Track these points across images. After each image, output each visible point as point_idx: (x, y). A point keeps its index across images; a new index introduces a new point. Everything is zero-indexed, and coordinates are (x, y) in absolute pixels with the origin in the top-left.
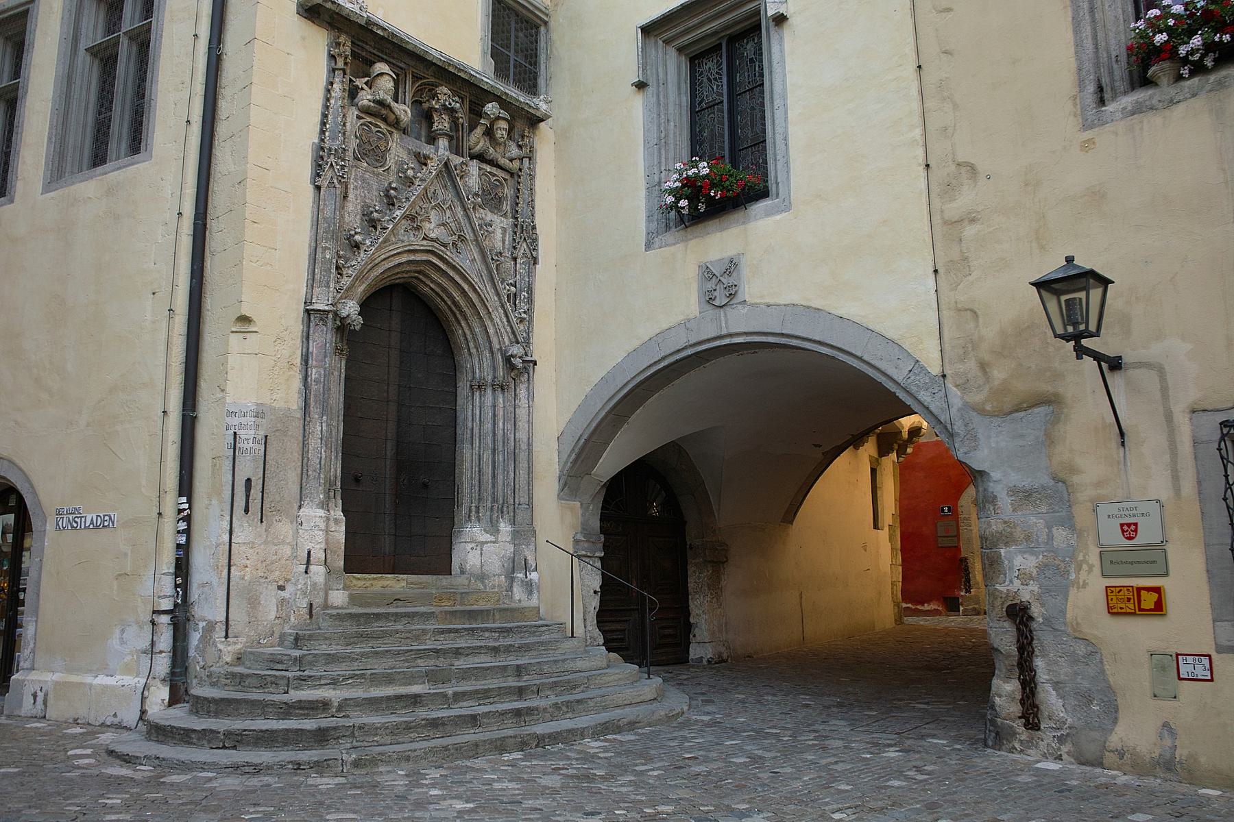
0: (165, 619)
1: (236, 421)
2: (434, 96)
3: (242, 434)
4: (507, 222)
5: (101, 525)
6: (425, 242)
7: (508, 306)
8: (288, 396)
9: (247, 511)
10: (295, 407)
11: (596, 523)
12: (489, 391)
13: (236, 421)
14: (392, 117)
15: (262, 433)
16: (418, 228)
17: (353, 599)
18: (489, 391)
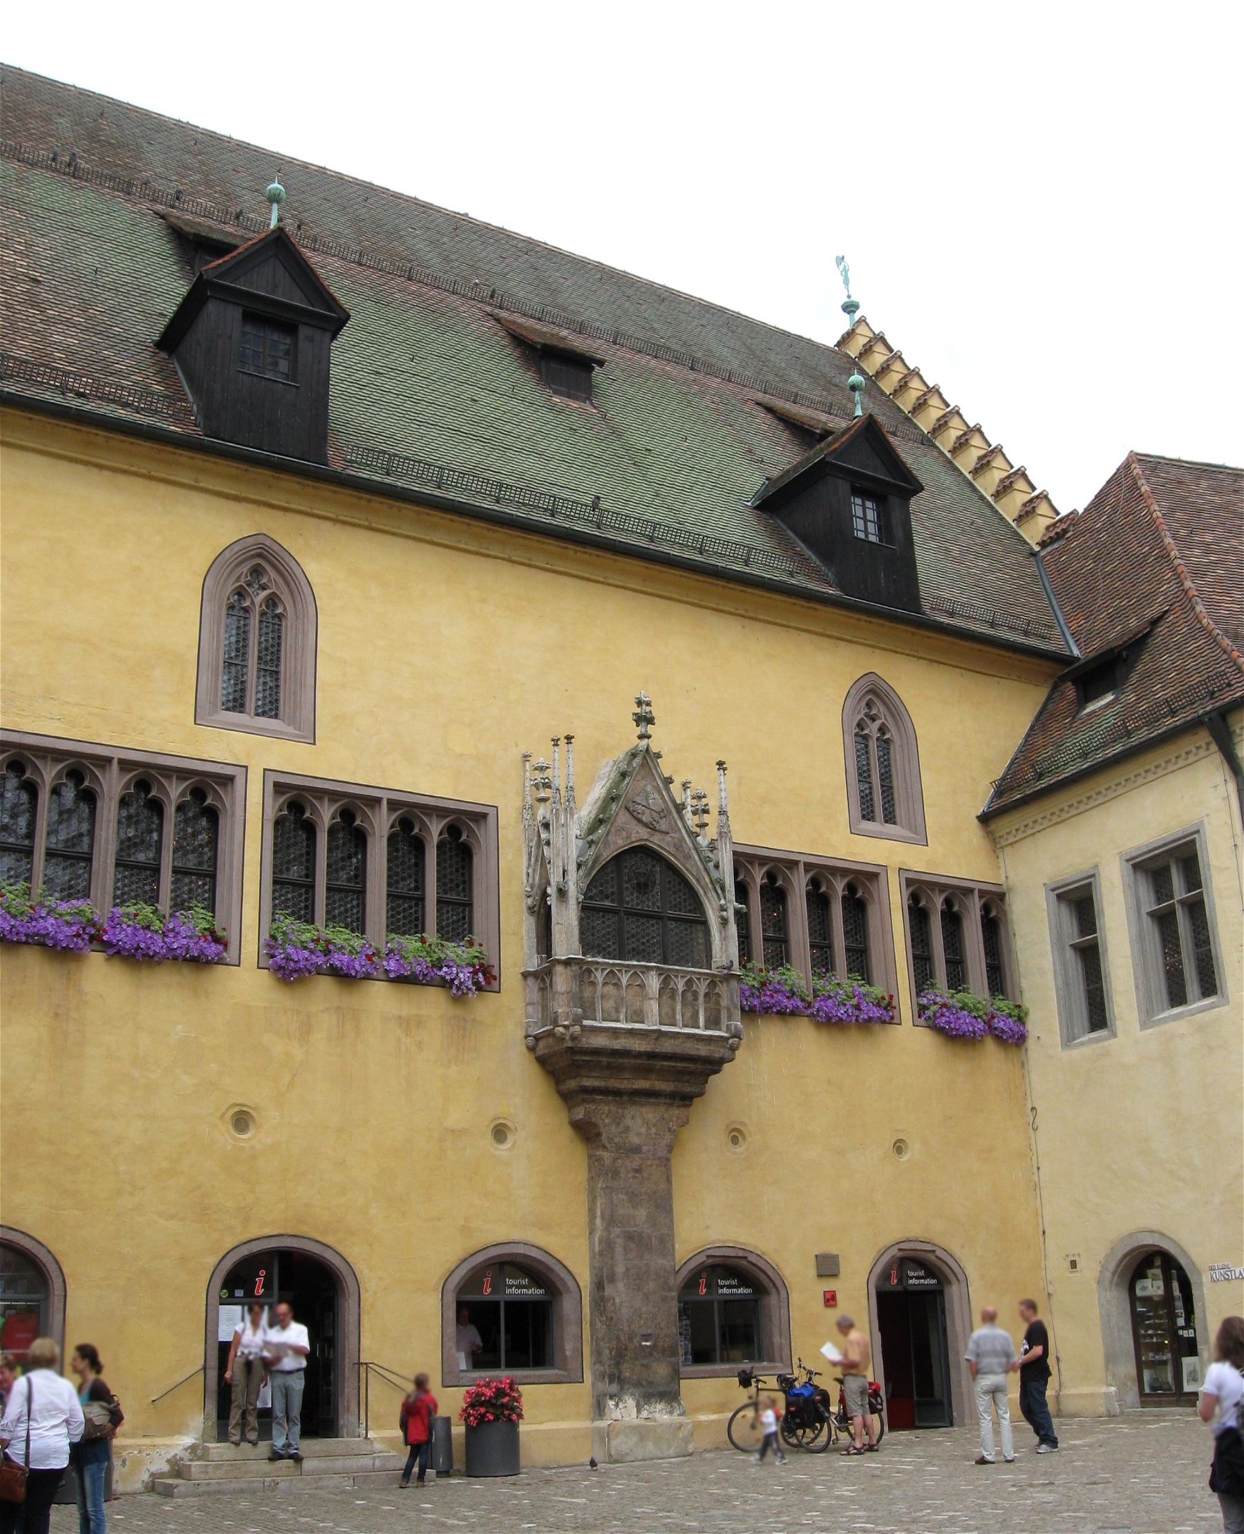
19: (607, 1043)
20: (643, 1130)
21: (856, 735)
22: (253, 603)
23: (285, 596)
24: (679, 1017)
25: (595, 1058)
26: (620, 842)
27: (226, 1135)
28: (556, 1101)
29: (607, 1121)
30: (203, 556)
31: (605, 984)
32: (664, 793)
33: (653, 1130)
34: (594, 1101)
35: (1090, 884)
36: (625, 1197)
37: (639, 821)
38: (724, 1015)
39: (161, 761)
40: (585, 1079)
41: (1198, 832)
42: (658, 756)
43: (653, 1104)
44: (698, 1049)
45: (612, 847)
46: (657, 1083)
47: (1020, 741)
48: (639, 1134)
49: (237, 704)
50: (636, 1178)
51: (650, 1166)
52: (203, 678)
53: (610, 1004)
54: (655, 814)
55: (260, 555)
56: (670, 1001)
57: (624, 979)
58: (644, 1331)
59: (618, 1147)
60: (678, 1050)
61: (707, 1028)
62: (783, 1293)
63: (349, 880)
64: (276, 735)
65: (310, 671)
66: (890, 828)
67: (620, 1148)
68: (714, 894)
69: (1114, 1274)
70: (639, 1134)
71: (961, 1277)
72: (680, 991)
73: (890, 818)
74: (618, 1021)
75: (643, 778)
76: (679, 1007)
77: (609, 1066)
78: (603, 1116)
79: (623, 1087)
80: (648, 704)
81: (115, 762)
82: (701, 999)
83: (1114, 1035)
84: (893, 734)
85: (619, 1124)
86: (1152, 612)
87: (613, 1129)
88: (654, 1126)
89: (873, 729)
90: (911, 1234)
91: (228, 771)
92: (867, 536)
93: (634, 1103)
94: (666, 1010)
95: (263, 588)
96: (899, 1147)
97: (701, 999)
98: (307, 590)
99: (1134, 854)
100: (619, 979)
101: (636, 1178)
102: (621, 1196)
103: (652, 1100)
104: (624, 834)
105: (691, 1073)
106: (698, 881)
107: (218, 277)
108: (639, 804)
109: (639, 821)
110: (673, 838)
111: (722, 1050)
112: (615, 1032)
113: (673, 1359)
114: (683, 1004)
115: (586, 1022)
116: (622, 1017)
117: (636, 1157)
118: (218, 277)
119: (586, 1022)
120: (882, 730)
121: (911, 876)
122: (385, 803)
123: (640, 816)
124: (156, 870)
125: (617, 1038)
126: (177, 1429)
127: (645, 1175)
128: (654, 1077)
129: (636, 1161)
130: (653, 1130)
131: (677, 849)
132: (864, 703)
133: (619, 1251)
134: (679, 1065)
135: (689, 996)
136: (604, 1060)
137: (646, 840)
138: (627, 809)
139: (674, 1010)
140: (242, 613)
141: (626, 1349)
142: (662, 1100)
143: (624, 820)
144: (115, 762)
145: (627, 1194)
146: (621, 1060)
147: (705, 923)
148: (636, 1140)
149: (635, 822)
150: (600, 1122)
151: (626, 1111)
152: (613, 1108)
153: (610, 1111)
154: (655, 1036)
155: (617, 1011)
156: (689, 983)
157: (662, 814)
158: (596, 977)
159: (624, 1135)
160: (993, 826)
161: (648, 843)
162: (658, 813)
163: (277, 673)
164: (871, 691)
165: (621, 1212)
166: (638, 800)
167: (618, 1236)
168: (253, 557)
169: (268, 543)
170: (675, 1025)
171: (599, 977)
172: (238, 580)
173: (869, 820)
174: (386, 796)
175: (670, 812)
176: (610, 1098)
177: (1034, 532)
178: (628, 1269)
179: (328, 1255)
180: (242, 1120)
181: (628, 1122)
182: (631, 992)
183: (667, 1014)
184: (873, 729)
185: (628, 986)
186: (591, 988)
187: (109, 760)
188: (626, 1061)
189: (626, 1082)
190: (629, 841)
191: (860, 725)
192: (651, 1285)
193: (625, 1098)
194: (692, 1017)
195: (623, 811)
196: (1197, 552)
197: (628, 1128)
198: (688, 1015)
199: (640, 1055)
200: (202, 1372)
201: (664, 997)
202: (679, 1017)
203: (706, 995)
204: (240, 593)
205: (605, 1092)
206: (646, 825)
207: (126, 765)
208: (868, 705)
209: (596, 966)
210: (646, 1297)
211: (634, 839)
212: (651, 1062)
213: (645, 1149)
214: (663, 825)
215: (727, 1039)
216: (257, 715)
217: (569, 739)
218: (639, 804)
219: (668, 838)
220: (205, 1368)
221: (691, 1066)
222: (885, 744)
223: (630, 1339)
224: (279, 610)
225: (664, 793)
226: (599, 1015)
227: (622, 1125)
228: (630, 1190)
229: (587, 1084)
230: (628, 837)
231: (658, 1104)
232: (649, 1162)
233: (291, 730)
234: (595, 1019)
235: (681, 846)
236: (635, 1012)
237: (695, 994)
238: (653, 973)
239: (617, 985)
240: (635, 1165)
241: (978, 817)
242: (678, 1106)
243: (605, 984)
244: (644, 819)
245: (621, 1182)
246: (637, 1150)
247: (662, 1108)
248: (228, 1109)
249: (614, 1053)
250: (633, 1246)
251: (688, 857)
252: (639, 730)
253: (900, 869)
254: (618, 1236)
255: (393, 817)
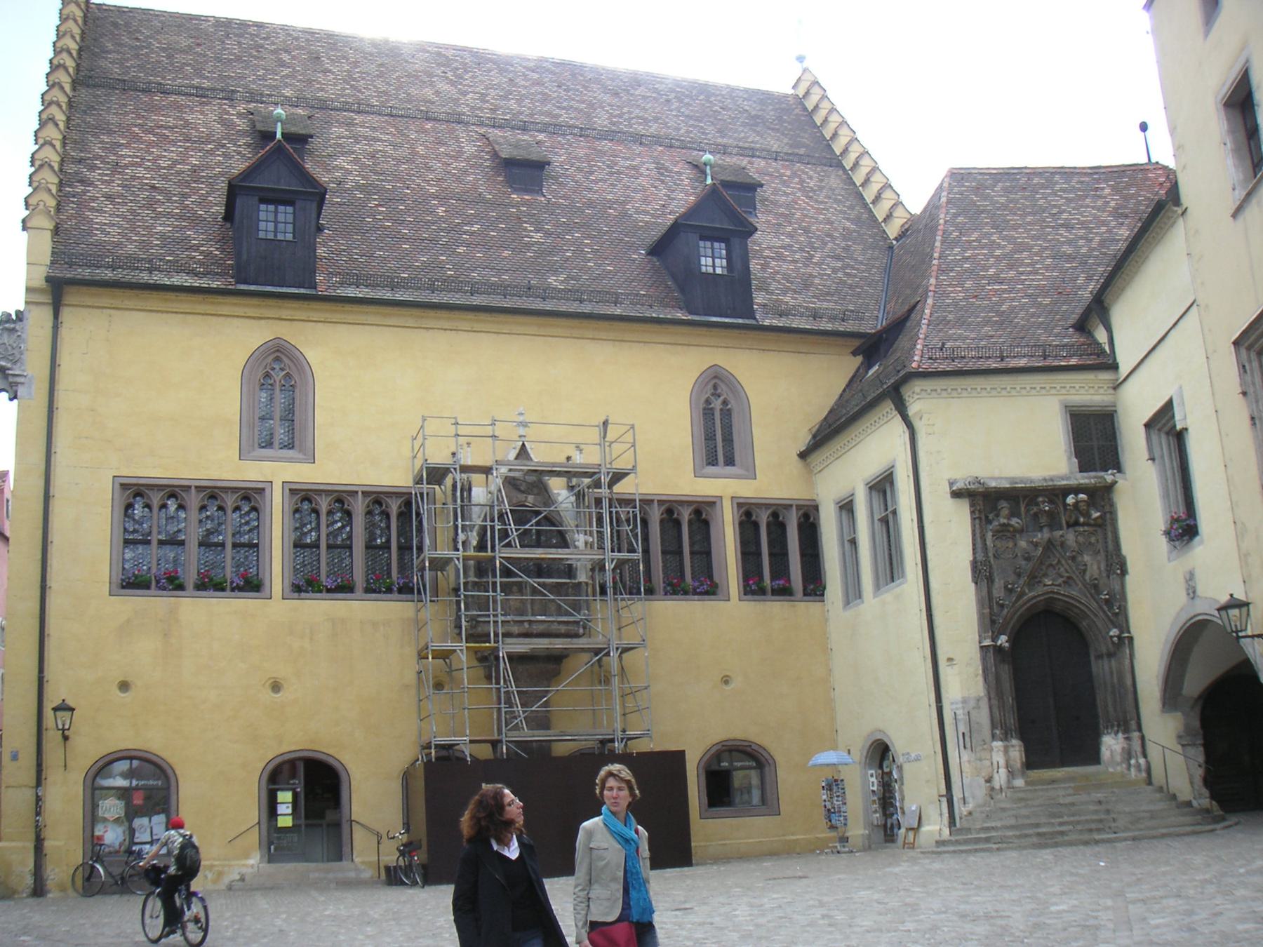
0: (944, 800)
1: (954, 706)
2: (1037, 504)
3: (958, 712)
4: (1101, 557)
5: (917, 759)
6: (1046, 588)
7: (1105, 608)
8: (977, 687)
9: (965, 747)
10: (982, 694)
11: (1196, 723)
12: (1105, 658)
13: (954, 706)
14: (1011, 529)
15: (966, 711)
16: (1040, 582)
17: (1027, 783)
18: (1105, 658)
21: (704, 409)
22: (275, 381)
23: (296, 376)
27: (268, 696)
30: (241, 358)
35: (852, 501)
39: (219, 484)
41: (893, 466)
47: (837, 397)
49: (269, 445)
52: (244, 430)
55: (278, 351)
63: (343, 540)
64: (290, 460)
65: (311, 419)
66: (729, 469)
69: (866, 758)
71: (771, 761)
73: (730, 461)
81: (193, 488)
83: (863, 602)
84: (733, 404)
86: (913, 302)
89: (717, 404)
90: (731, 736)
91: (260, 485)
92: (714, 270)
95: (282, 369)
96: (726, 681)
98: (307, 368)
99: (870, 480)
107: (242, 181)
118: (242, 181)
120: (725, 403)
121: (741, 501)
122: (360, 493)
124: (223, 545)
126: (247, 857)
132: (710, 386)
140: (269, 387)
144: (193, 488)
160: (809, 460)
163: (293, 421)
164: (715, 377)
168: (278, 351)
169: (283, 342)
172: (265, 368)
173: (713, 465)
174: (360, 489)
177: (893, 230)
179: (331, 761)
180: (276, 687)
184: (717, 404)
187: (190, 487)
191: (708, 402)
196: (957, 250)
200: (257, 826)
204: (267, 375)
207: (199, 489)
208: (715, 387)
216: (281, 448)
220: (259, 823)
222: (727, 414)
224: (293, 383)
233: (301, 456)
241: (798, 455)
244: (522, 488)
248: (267, 681)
253: (732, 497)
255: (367, 501)
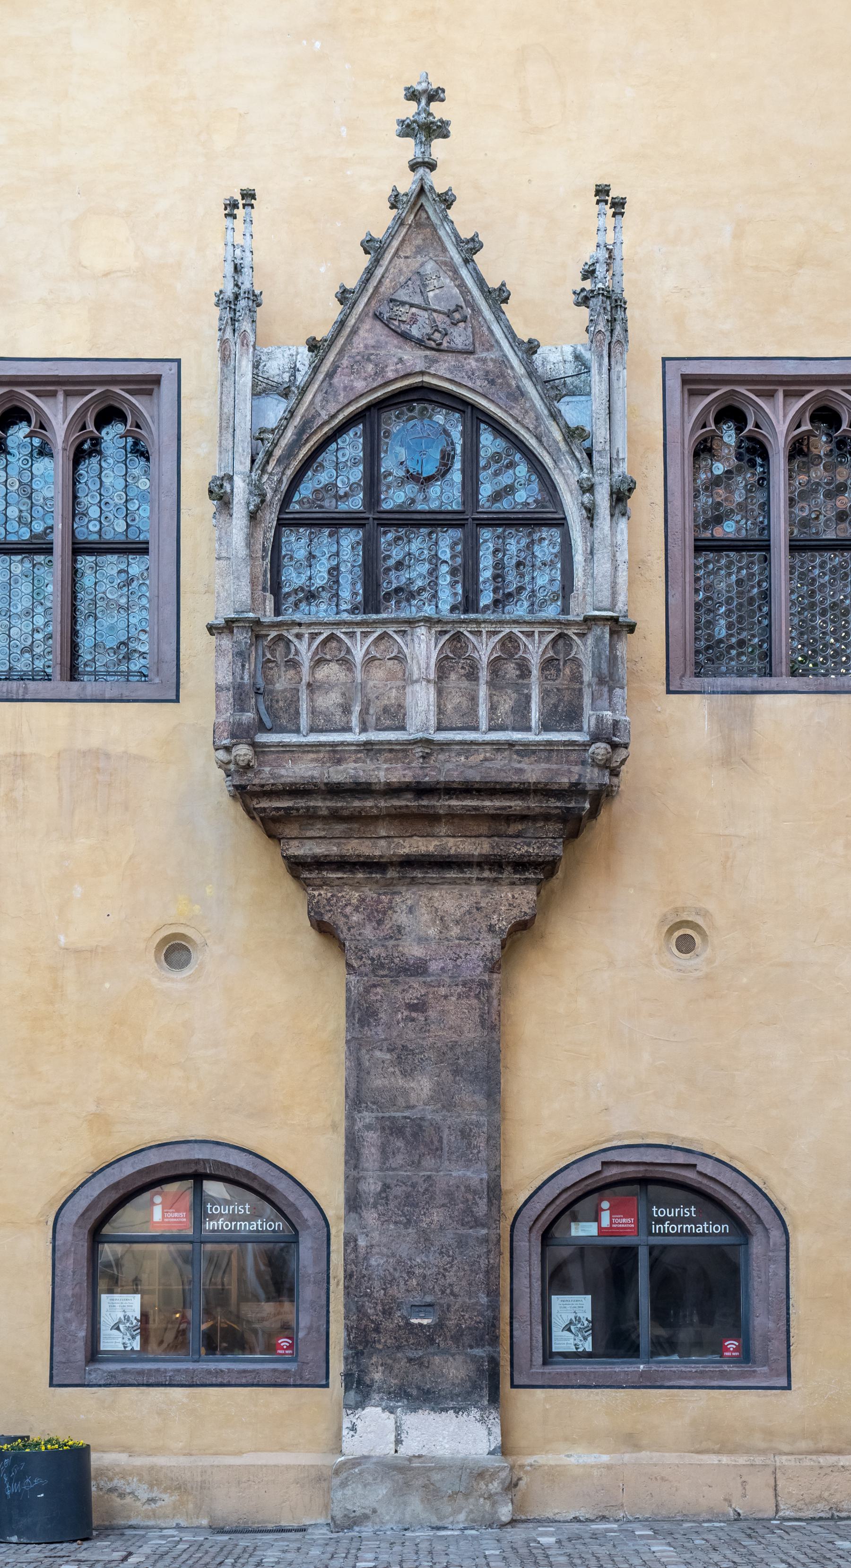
19: (316, 773)
20: (432, 932)
24: (483, 711)
25: (301, 803)
26: (360, 385)
28: (289, 885)
29: (355, 918)
31: (318, 662)
32: (464, 272)
33: (455, 931)
34: (325, 883)
36: (388, 1056)
37: (405, 336)
38: (587, 701)
40: (296, 843)
42: (447, 200)
43: (453, 882)
44: (521, 771)
45: (342, 399)
46: (451, 842)
48: (422, 940)
50: (413, 1020)
51: (446, 997)
53: (329, 701)
54: (439, 318)
56: (465, 684)
57: (358, 654)
58: (417, 1299)
59: (377, 965)
60: (474, 776)
61: (546, 727)
62: (776, 1234)
67: (382, 966)
68: (573, 464)
70: (422, 940)
72: (485, 660)
74: (348, 729)
75: (419, 250)
76: (483, 691)
77: (335, 816)
78: (348, 910)
79: (377, 853)
80: (435, 95)
82: (535, 672)
85: (380, 922)
87: (368, 932)
88: (457, 922)
93: (413, 881)
94: (455, 700)
97: (535, 672)
100: (348, 651)
101: (413, 1020)
102: (378, 1054)
103: (452, 874)
104: (370, 368)
105: (523, 818)
106: (539, 439)
108: (403, 303)
109: (405, 336)
110: (484, 361)
111: (576, 769)
112: (336, 752)
113: (478, 1352)
114: (491, 684)
115: (263, 738)
116: (355, 721)
117: (415, 982)
119: (263, 738)
123: (403, 327)
125: (339, 762)
127: (432, 1014)
128: (443, 829)
129: (415, 989)
130: (455, 931)
131: (492, 382)
133: (370, 1154)
134: (487, 803)
135: (511, 670)
136: (321, 804)
137: (422, 373)
138: (378, 317)
139: (474, 699)
141: (377, 1330)
142: (475, 874)
143: (371, 342)
145: (390, 1051)
146: (357, 803)
147: (561, 523)
148: (414, 951)
149: (396, 341)
150: (341, 921)
151: (398, 899)
152: (369, 893)
153: (362, 900)
154: (418, 751)
155: (346, 710)
156: (509, 644)
157: (457, 316)
158: (297, 652)
159: (392, 942)
161: (427, 379)
162: (449, 314)
165: (378, 1082)
166: (402, 295)
167: (368, 1127)
170: (476, 729)
171: (304, 650)
175: (476, 311)
176: (360, 875)
178: (386, 1187)
181: (402, 918)
182: (378, 674)
183: (456, 709)
185: (370, 660)
186: (292, 672)
188: (369, 803)
189: (383, 843)
190: (380, 381)
192: (437, 1216)
193: (391, 874)
194: (514, 711)
195: (368, 323)
197: (400, 929)
198: (506, 705)
199: (393, 790)
201: (453, 676)
202: (483, 711)
203: (548, 664)
205: (343, 864)
206: (420, 343)
209: (296, 630)
210: (425, 1239)
211: (391, 375)
212: (425, 803)
213: (434, 966)
214: (459, 337)
215: (586, 745)
217: (249, 195)
218: (403, 303)
219: (472, 363)
221: (516, 804)
223: (387, 1313)
225: (464, 272)
226: (304, 722)
227: (388, 924)
228: (399, 1043)
229: (301, 852)
230: (380, 371)
231: (467, 882)
232: (443, 991)
234: (297, 731)
235: (502, 375)
236: (386, 710)
237: (524, 670)
238: (422, 631)
239: (346, 662)
240: (411, 996)
242: (513, 884)
243: (318, 662)
244: (415, 332)
245: (380, 1029)
246: (419, 969)
247: (477, 889)
249: (334, 790)
250: (400, 1143)
251: (519, 394)
252: (409, 148)
254: (368, 1127)
